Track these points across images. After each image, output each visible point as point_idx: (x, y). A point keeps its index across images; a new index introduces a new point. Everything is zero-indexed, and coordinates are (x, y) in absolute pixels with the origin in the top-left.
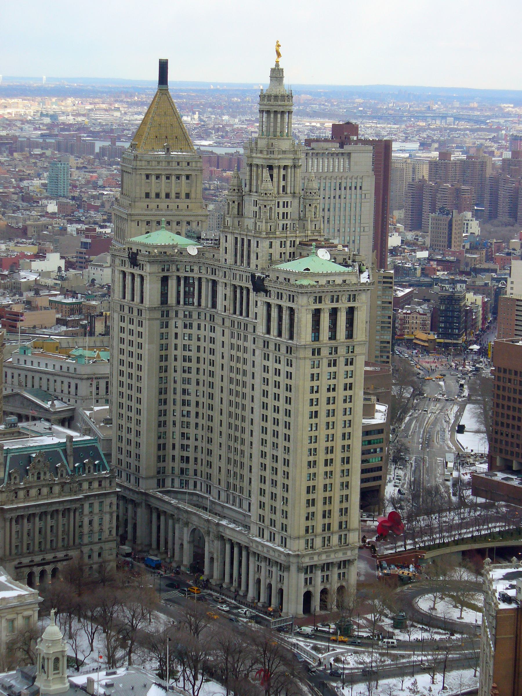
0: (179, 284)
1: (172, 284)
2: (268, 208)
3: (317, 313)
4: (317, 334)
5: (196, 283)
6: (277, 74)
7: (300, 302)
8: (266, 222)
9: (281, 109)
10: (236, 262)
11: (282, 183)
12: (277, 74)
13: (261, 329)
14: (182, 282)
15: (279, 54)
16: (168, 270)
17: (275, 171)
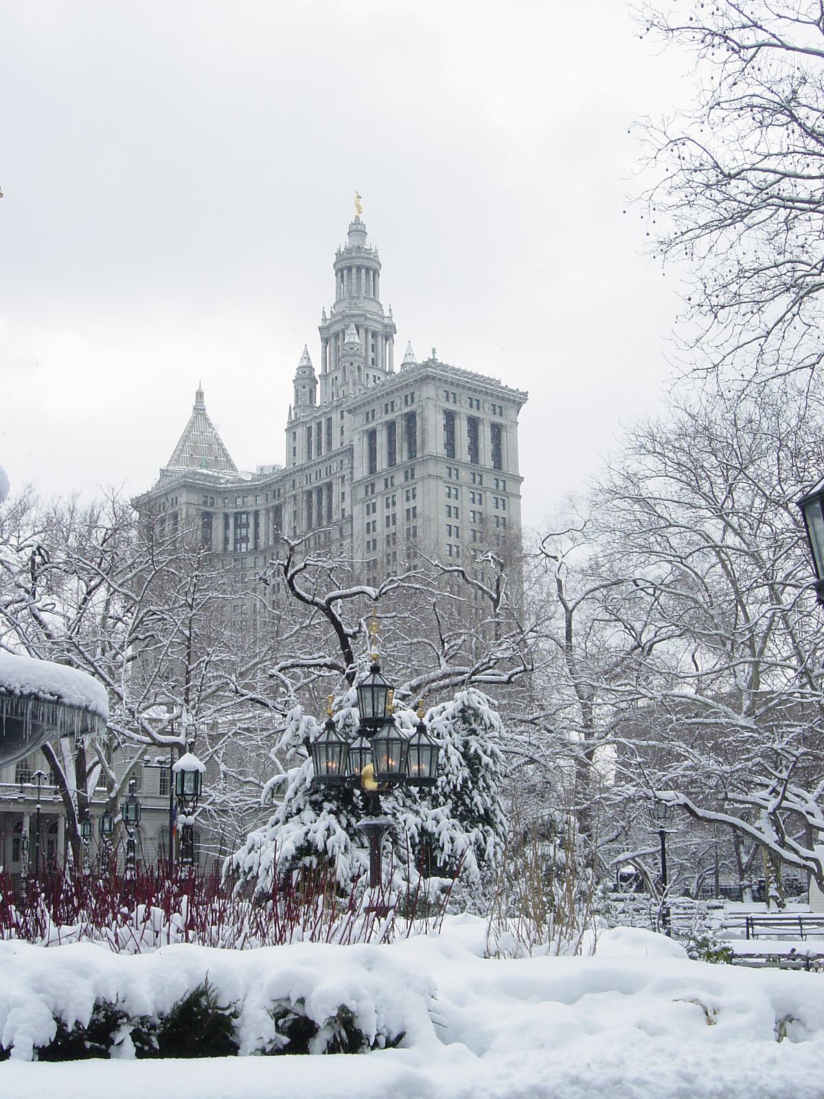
0: (227, 526)
1: (218, 524)
2: (356, 365)
3: (450, 416)
4: (450, 453)
5: (251, 520)
6: (357, 230)
7: (424, 395)
8: (354, 384)
9: (366, 263)
10: (310, 458)
11: (371, 355)
12: (357, 230)
13: (361, 471)
14: (231, 521)
15: (359, 207)
16: (212, 504)
17: (362, 331)
